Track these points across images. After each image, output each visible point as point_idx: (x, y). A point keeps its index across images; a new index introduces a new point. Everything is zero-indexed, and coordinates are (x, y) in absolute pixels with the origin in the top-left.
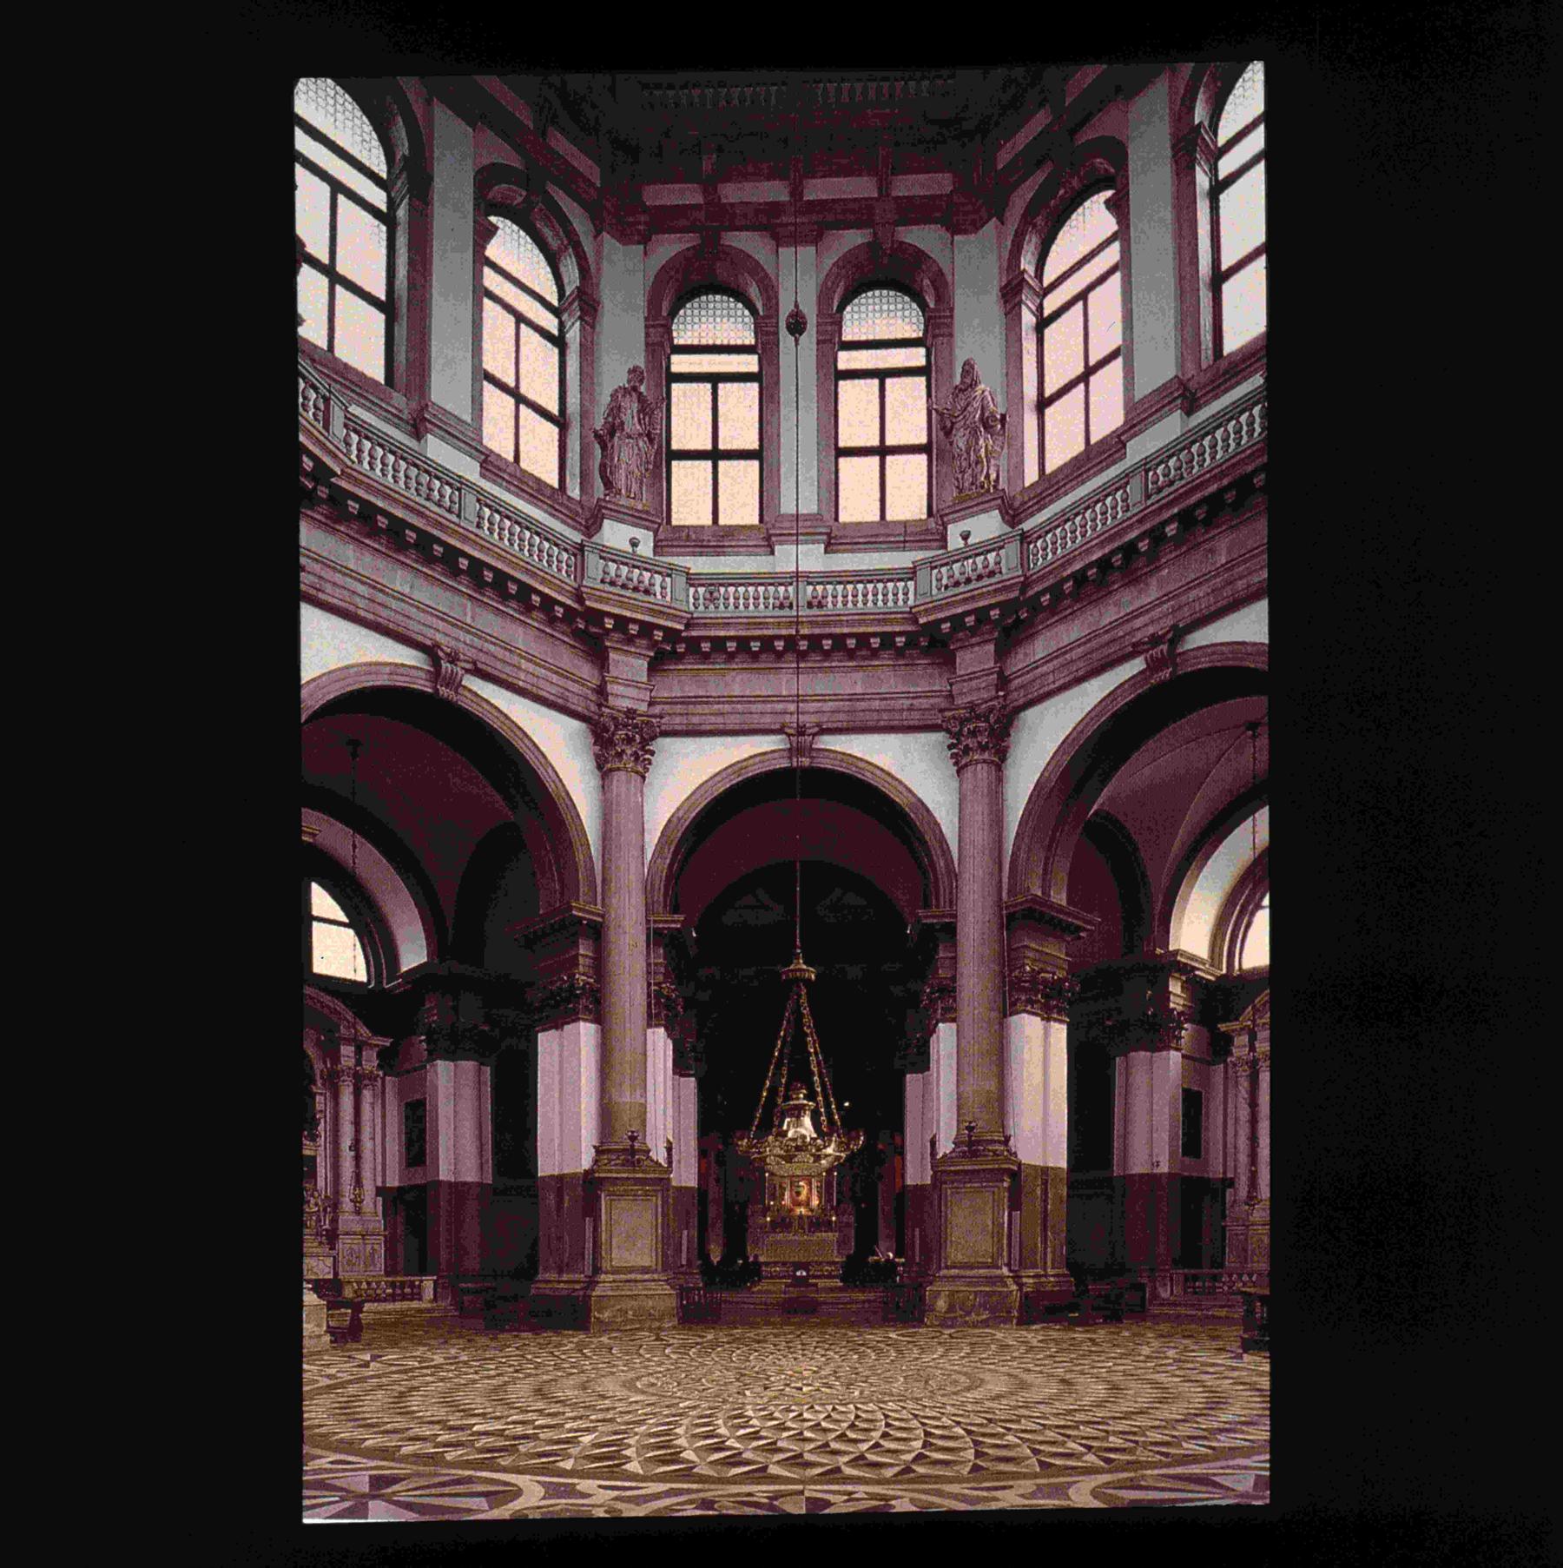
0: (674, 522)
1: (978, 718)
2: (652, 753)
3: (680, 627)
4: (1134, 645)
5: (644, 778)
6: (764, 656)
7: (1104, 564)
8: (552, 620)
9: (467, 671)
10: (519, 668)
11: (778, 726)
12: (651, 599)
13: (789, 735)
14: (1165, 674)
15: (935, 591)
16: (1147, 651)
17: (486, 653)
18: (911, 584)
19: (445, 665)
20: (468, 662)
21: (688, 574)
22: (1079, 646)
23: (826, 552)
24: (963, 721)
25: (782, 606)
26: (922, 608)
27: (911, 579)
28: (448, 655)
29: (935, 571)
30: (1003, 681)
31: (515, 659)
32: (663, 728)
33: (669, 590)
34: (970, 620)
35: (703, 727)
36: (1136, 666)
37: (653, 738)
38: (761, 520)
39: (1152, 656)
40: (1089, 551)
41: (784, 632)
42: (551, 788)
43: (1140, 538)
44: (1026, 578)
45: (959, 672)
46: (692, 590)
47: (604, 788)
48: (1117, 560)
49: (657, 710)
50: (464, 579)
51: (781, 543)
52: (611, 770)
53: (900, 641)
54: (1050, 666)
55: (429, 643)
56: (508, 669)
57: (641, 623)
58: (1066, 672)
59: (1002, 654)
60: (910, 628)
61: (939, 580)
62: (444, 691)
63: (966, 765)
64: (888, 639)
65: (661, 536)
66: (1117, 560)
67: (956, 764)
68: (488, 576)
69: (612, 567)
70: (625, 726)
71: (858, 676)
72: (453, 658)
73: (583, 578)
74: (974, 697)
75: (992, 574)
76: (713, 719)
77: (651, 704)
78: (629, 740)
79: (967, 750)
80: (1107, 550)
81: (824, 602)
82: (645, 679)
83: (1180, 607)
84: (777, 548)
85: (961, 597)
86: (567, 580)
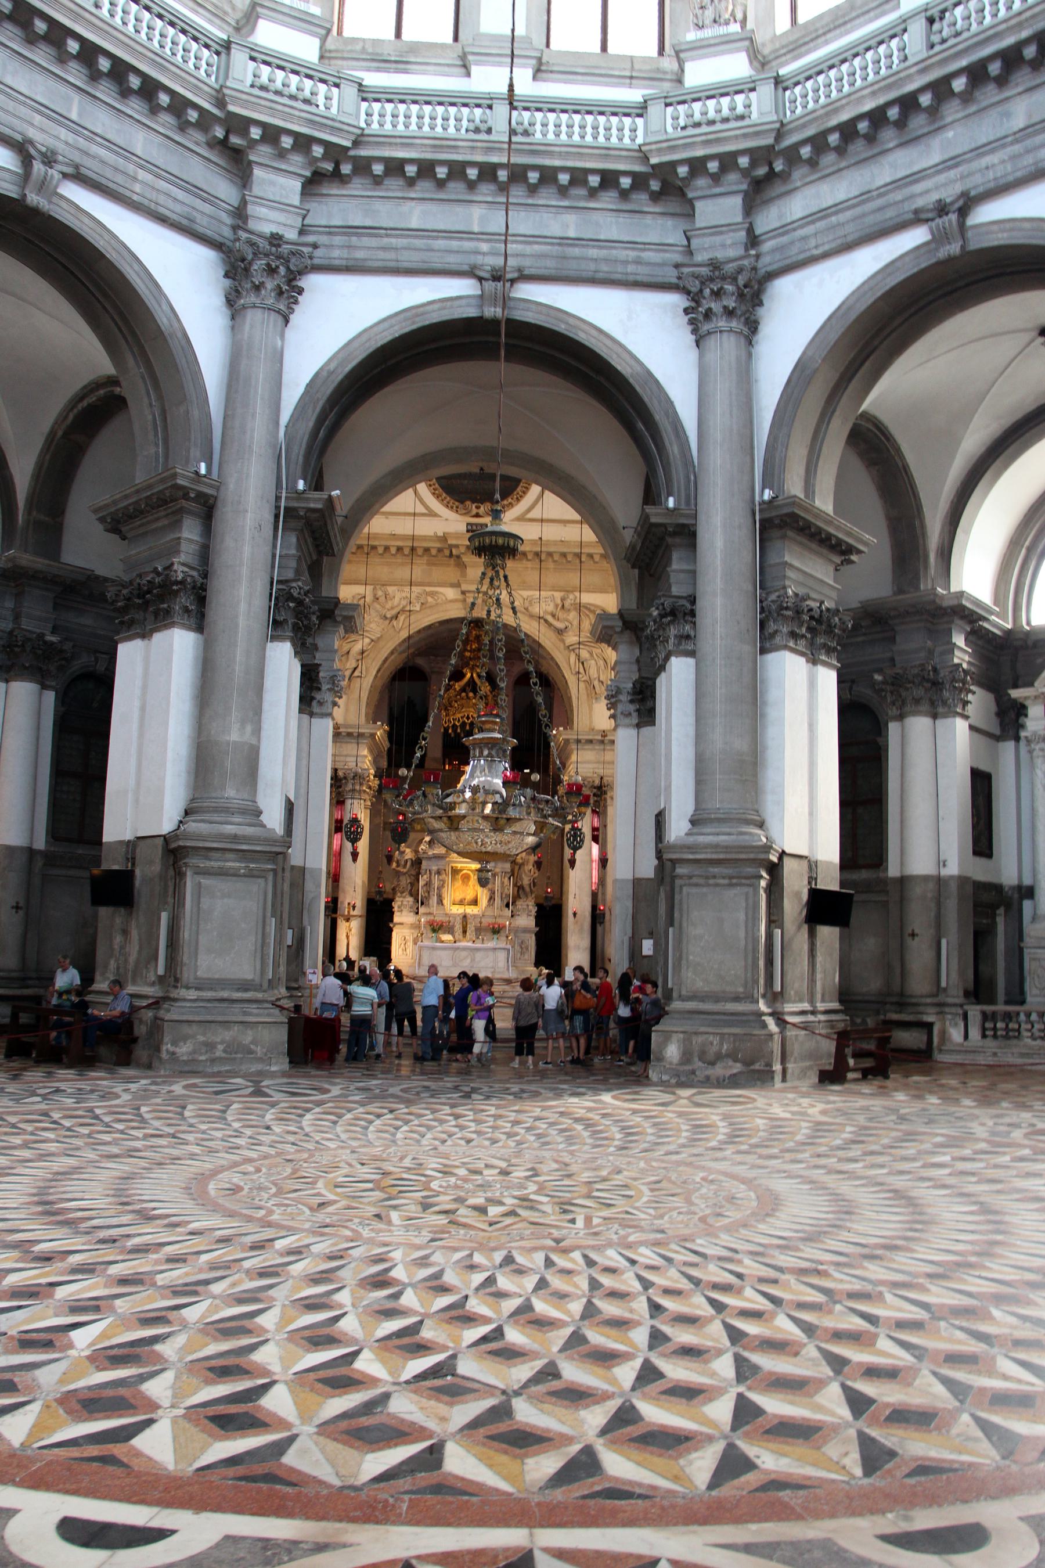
0: (346, 33)
1: (723, 278)
2: (300, 291)
3: (348, 144)
4: (916, 212)
5: (287, 321)
6: (451, 185)
7: (877, 117)
8: (183, 126)
9: (65, 176)
10: (135, 179)
11: (466, 268)
12: (313, 109)
13: (480, 279)
14: (954, 248)
15: (670, 129)
16: (932, 220)
17: (94, 157)
18: (639, 121)
19: (38, 167)
20: (67, 164)
21: (360, 85)
22: (849, 208)
23: (535, 78)
24: (704, 281)
25: (477, 130)
26: (654, 147)
27: (640, 116)
28: (44, 155)
29: (670, 109)
30: (753, 240)
31: (131, 168)
32: (316, 261)
33: (335, 102)
34: (713, 166)
35: (370, 264)
36: (916, 237)
37: (302, 272)
38: (456, 39)
39: (938, 225)
40: (860, 101)
41: (479, 158)
42: (163, 321)
43: (922, 90)
44: (782, 124)
45: (698, 225)
46: (364, 105)
47: (233, 328)
48: (893, 113)
49: (310, 239)
50: (73, 65)
51: (478, 63)
52: (244, 307)
53: (626, 182)
54: (809, 230)
55: (19, 138)
56: (120, 179)
57: (296, 135)
58: (831, 237)
59: (749, 209)
60: (638, 168)
61: (675, 118)
62: (33, 199)
63: (709, 333)
64: (609, 179)
65: (330, 44)
66: (893, 113)
67: (694, 331)
68: (104, 64)
69: (265, 70)
70: (267, 255)
71: (571, 218)
72: (49, 159)
73: (227, 77)
74: (720, 255)
75: (742, 117)
76: (381, 255)
77: (302, 232)
78: (272, 271)
79: (708, 315)
80: (881, 100)
81: (531, 130)
82: (297, 203)
83: (970, 174)
84: (474, 69)
85: (703, 138)
86: (207, 80)
